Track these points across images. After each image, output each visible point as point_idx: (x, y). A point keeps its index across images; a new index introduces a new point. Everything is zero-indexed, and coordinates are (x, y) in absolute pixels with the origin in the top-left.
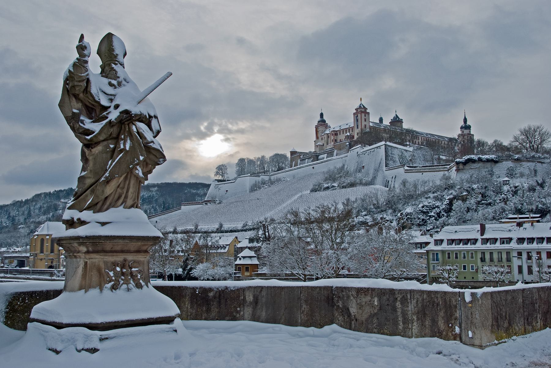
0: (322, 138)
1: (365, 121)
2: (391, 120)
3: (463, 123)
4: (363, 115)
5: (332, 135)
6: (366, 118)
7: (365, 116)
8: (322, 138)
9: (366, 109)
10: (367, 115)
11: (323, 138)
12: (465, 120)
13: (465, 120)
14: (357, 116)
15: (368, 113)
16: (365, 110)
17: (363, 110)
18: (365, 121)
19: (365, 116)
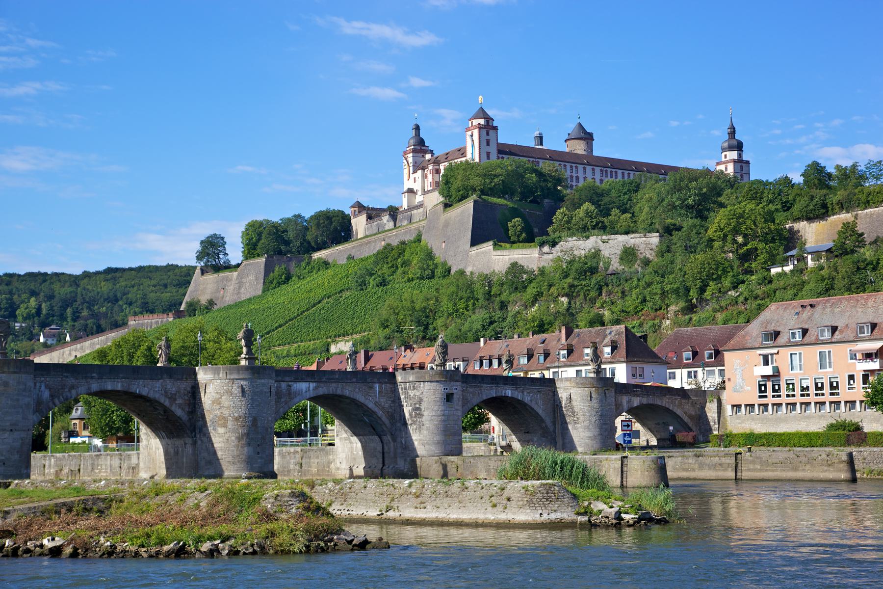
0: (415, 178)
1: (488, 144)
2: (569, 134)
3: (727, 137)
4: (484, 131)
5: (430, 173)
6: (488, 138)
7: (488, 134)
8: (415, 178)
9: (488, 119)
10: (491, 132)
11: (417, 179)
12: (732, 133)
13: (732, 133)
14: (472, 136)
15: (496, 128)
16: (488, 122)
17: (482, 122)
18: (488, 144)
19: (488, 134)
